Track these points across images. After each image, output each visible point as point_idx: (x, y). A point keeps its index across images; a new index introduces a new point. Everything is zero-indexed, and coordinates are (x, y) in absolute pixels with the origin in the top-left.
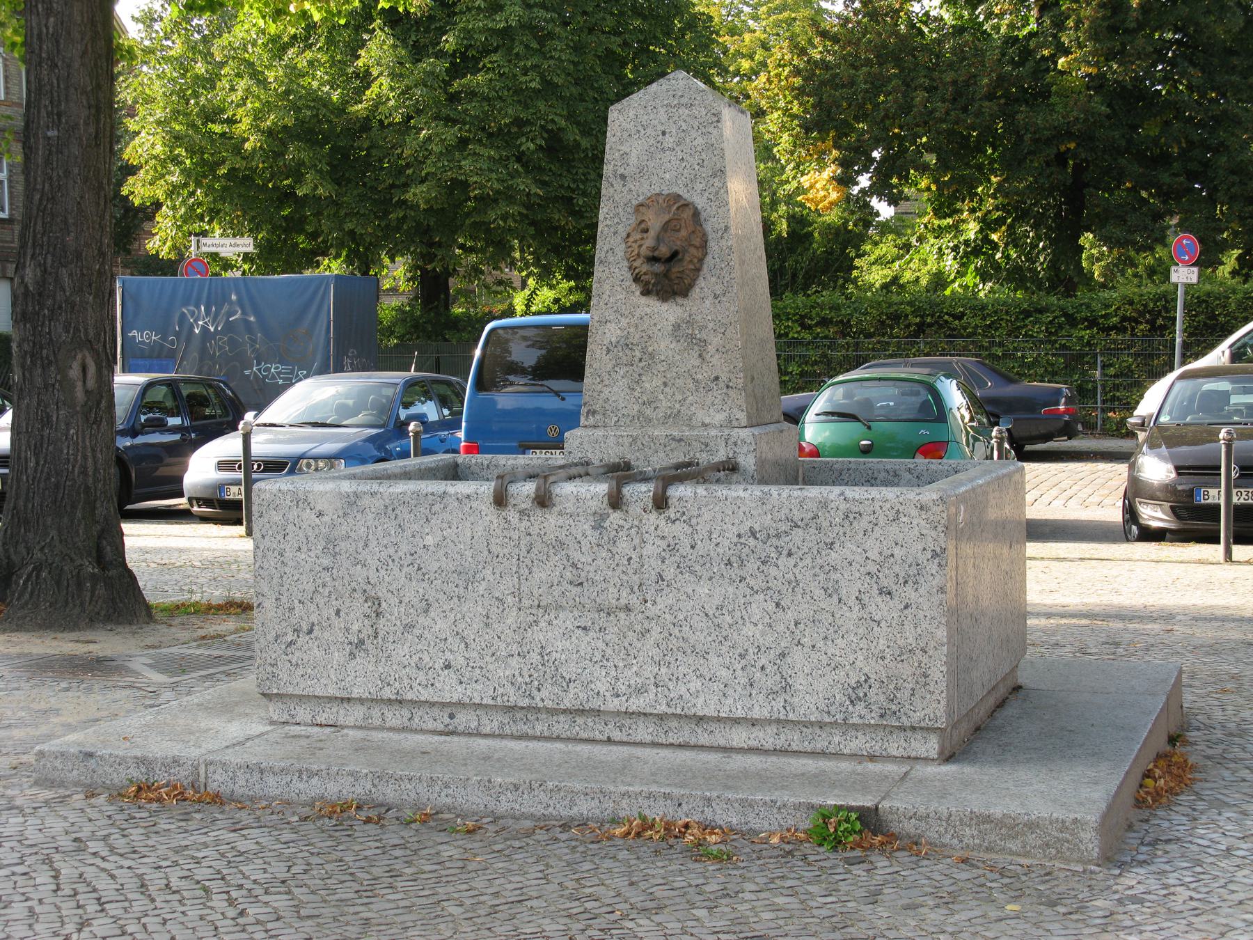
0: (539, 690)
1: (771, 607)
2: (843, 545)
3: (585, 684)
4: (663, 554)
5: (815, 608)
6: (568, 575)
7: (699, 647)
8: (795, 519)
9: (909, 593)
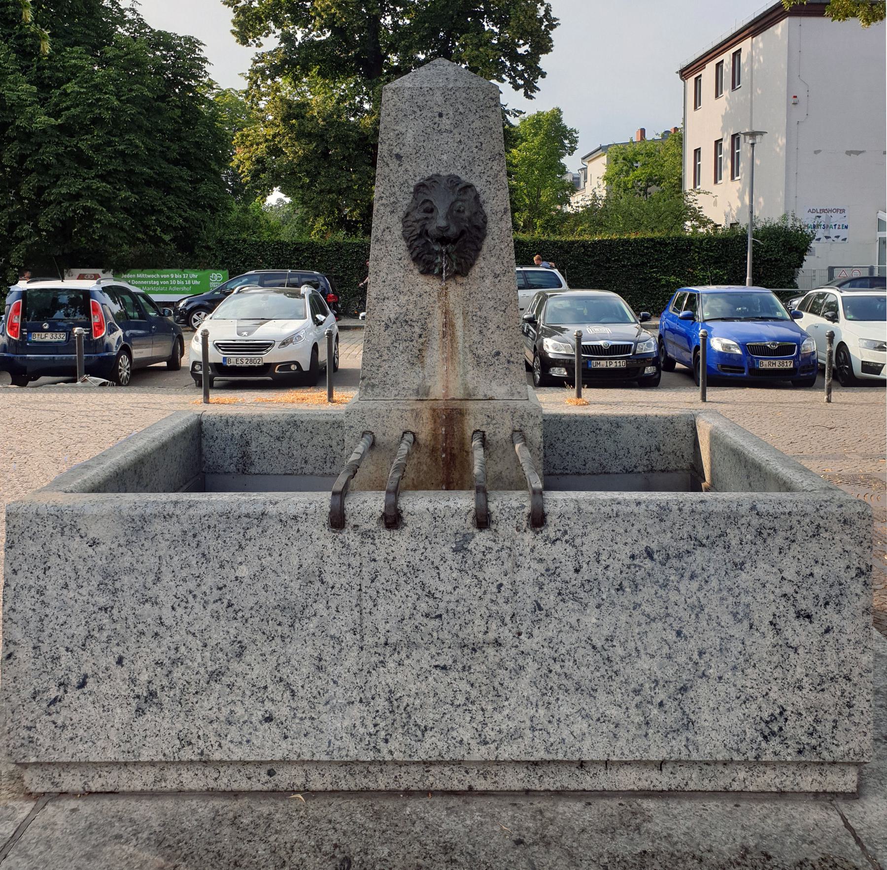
0: (387, 741)
1: (671, 636)
2: (754, 563)
3: (445, 732)
4: (541, 579)
5: (723, 636)
6: (423, 606)
7: (585, 684)
8: (699, 536)
9: (830, 615)
